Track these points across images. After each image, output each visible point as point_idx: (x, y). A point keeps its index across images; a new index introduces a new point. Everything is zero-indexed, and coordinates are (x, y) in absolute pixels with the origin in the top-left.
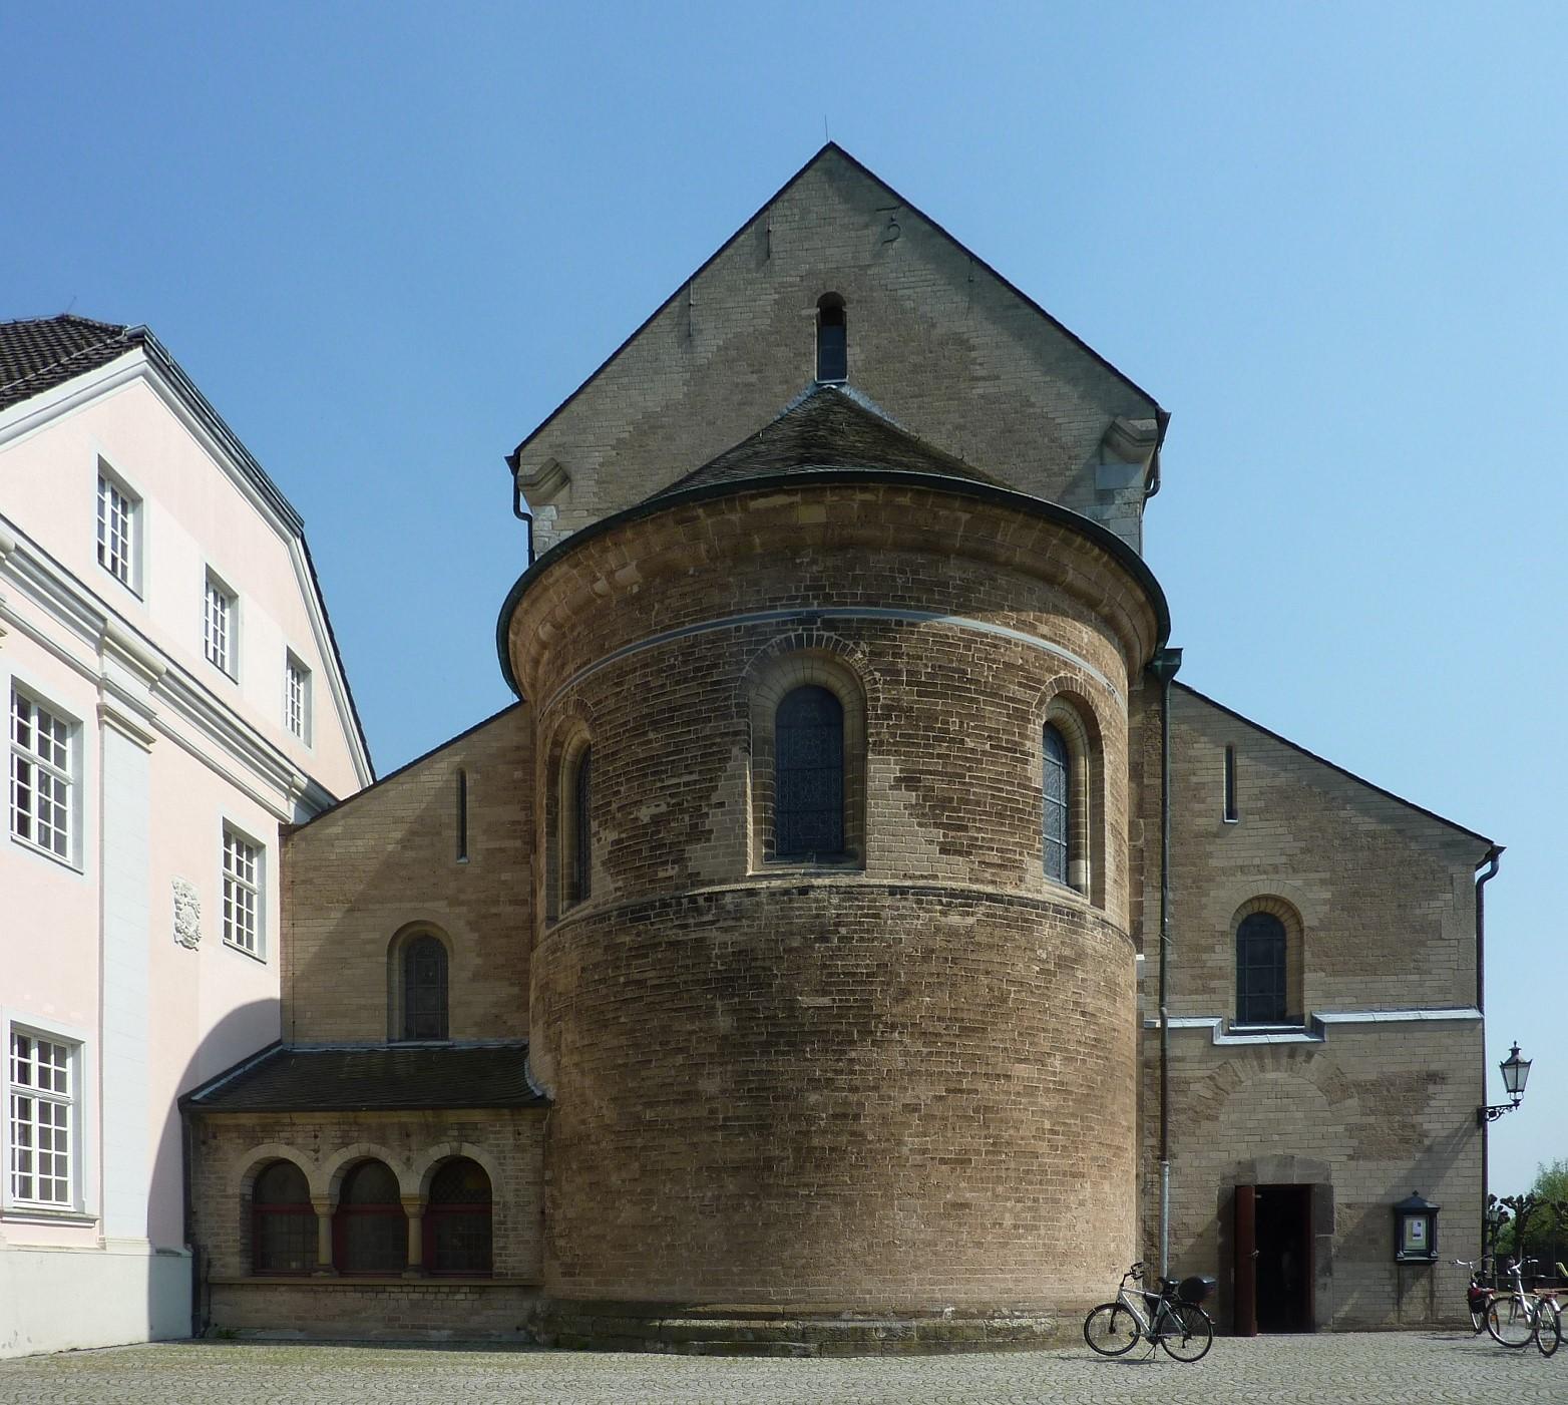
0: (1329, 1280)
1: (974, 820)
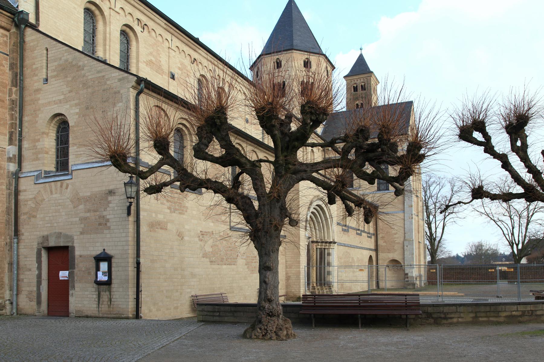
0: (73, 292)
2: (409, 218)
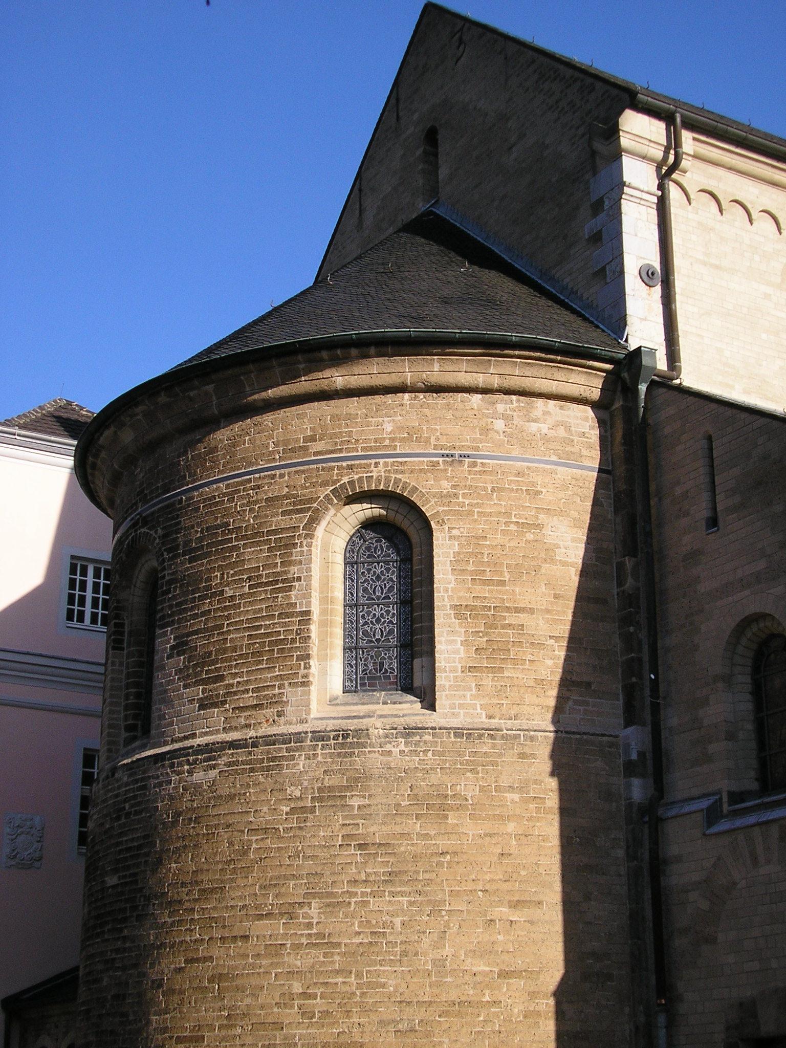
1: (230, 667)
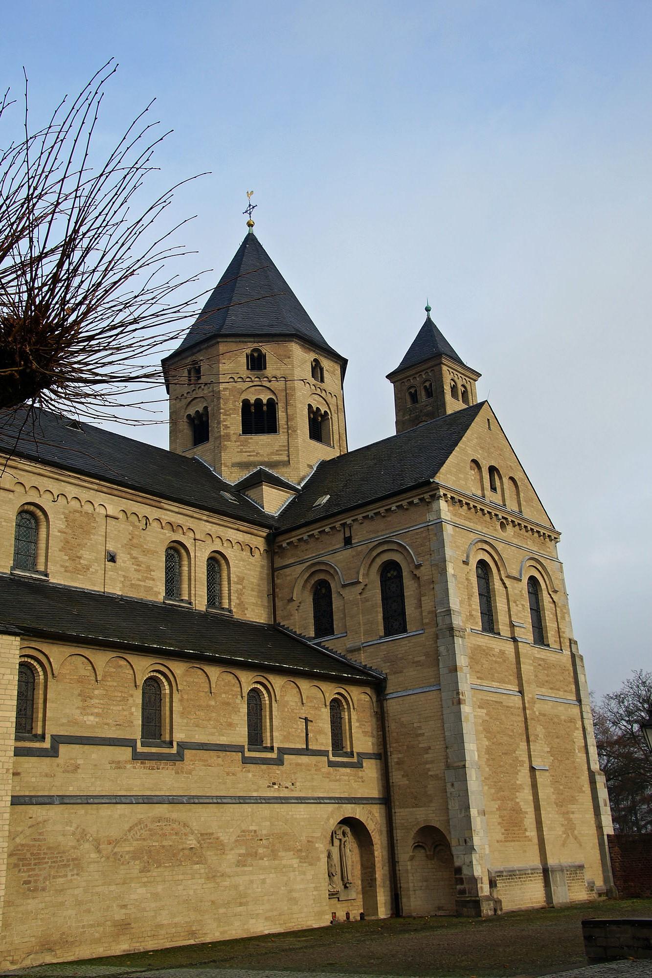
2: (453, 703)
